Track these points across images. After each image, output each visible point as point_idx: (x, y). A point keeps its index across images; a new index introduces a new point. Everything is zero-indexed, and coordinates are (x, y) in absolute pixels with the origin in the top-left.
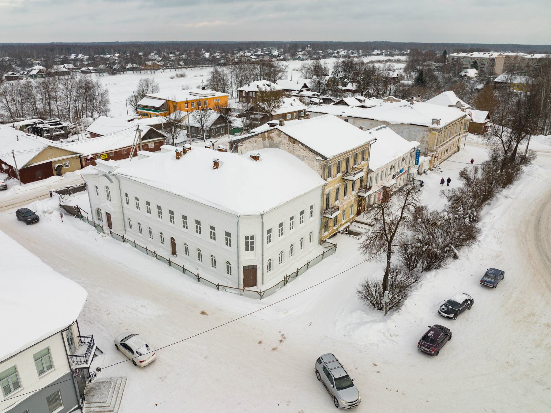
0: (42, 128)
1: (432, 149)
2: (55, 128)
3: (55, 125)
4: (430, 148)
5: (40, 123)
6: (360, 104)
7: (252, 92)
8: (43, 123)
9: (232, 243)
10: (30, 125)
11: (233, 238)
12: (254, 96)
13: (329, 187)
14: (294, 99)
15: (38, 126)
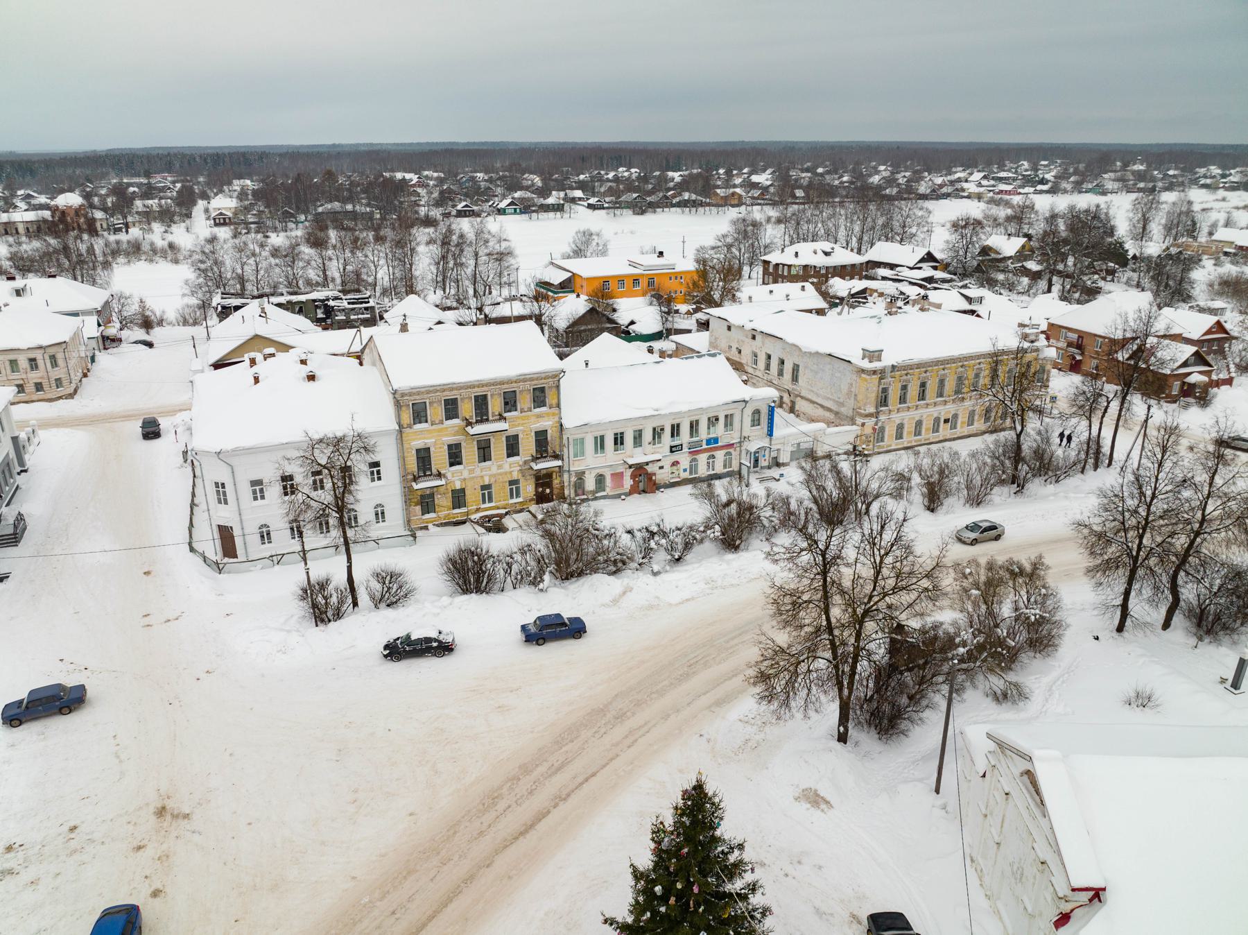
0: (333, 307)
1: (863, 411)
2: (361, 309)
3: (362, 303)
4: (860, 408)
5: (336, 298)
6: (967, 307)
7: (784, 265)
8: (341, 299)
9: (228, 498)
10: (320, 301)
11: (229, 489)
12: (786, 274)
13: (425, 438)
14: (803, 287)
15: (331, 303)
